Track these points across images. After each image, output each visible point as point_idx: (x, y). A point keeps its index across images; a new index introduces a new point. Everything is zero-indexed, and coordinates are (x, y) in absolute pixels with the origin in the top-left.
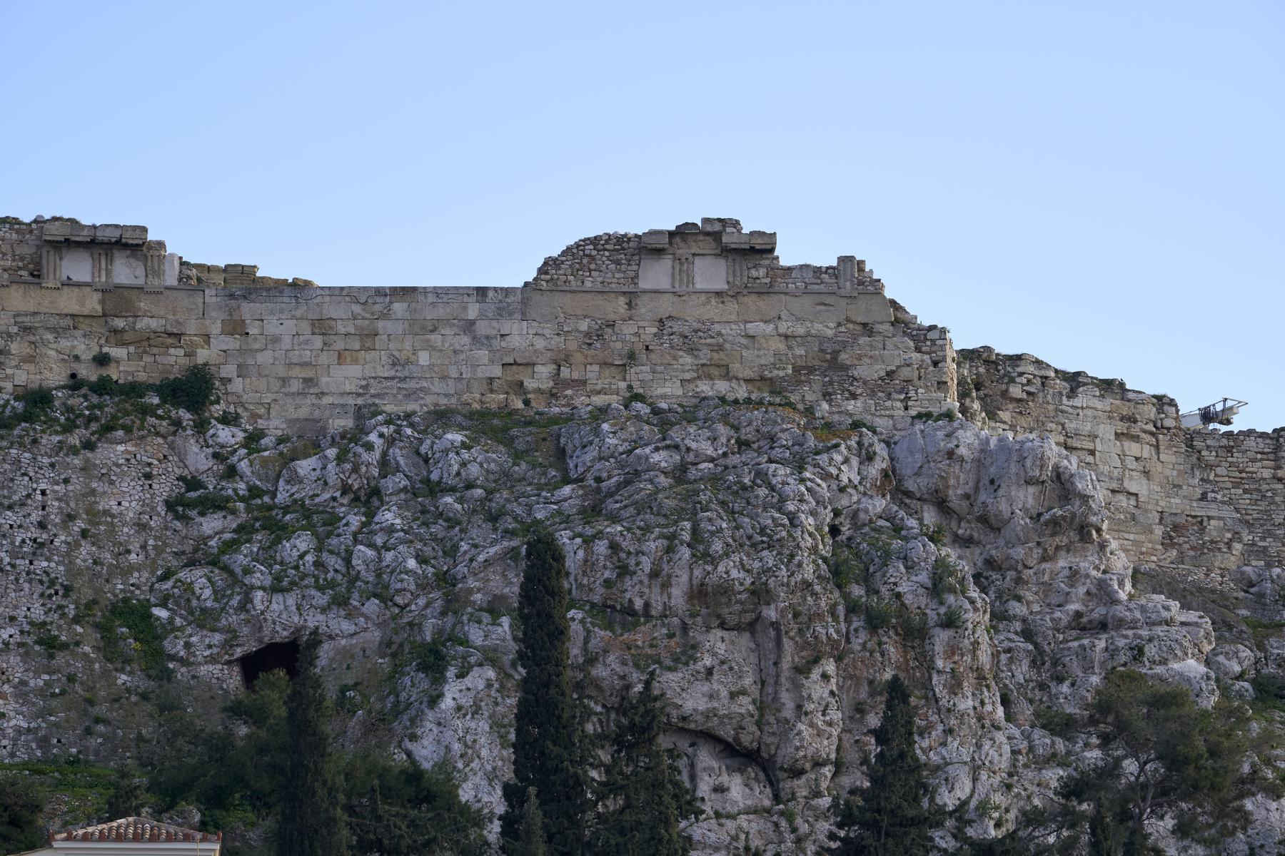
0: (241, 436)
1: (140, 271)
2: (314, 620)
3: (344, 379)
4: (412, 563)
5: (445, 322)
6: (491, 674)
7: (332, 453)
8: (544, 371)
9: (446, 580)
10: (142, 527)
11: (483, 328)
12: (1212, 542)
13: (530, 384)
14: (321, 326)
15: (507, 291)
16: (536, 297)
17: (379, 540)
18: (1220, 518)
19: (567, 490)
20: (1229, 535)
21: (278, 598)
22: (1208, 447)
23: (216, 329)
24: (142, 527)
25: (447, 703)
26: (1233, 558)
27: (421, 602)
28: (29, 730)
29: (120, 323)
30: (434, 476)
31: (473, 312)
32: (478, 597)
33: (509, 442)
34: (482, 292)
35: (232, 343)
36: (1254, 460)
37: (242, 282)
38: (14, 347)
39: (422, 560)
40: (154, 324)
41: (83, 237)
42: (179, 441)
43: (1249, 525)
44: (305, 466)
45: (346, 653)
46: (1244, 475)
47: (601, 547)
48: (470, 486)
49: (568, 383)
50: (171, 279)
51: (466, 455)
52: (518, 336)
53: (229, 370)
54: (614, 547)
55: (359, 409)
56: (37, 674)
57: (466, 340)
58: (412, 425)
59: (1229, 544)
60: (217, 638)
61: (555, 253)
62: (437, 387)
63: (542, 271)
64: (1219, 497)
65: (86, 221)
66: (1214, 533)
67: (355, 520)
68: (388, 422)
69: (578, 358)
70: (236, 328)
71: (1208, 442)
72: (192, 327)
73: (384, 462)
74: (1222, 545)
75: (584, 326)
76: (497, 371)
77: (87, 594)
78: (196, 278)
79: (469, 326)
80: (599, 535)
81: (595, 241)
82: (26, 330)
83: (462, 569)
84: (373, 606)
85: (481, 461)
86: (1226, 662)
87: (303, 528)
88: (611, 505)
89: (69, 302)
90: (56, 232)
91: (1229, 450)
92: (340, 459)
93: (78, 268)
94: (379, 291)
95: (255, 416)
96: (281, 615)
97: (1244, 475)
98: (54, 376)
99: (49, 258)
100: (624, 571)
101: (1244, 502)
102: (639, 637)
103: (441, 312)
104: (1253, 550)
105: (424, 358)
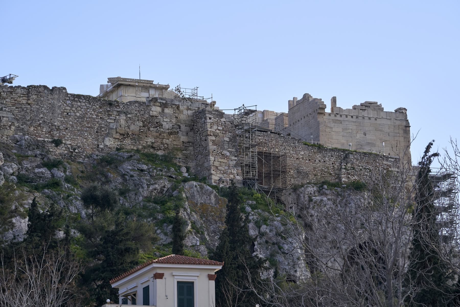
12: (4, 125)
18: (7, 117)
20: (10, 123)
22: (4, 91)
26: (11, 132)
36: (20, 97)
43: (18, 120)
46: (16, 102)
59: (10, 127)
64: (7, 109)
66: (5, 122)
71: (4, 90)
74: (7, 127)
86: (8, 169)
91: (11, 93)
97: (16, 102)
101: (16, 112)
104: (18, 129)
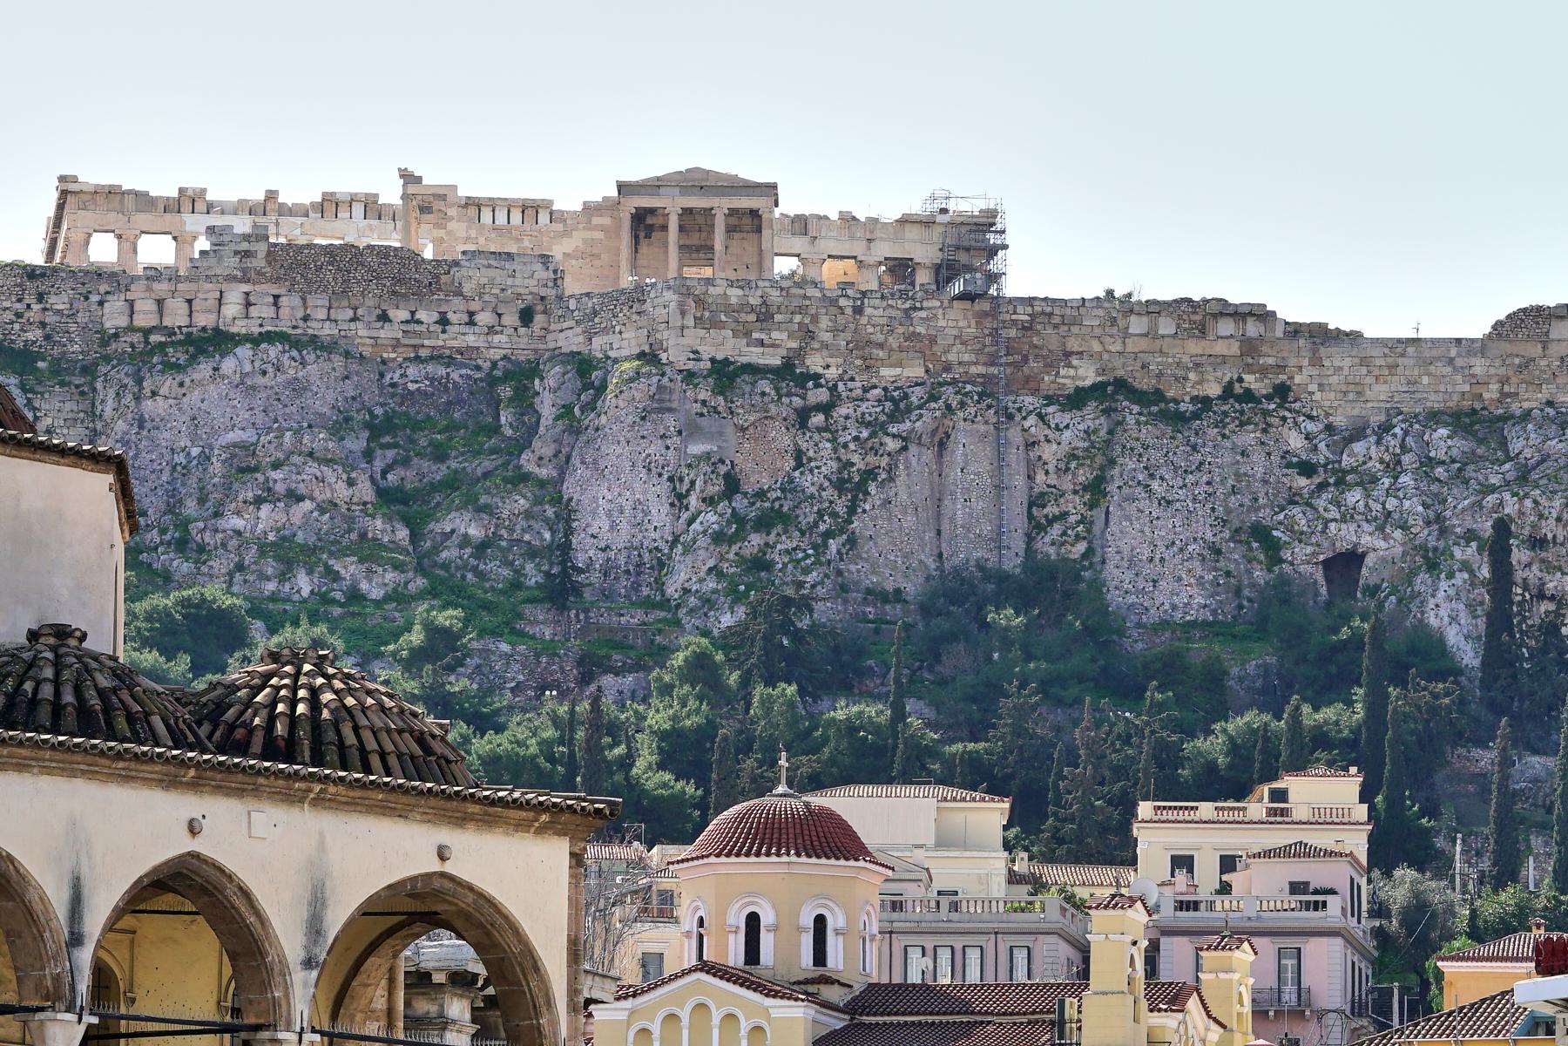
0: (1321, 426)
1: (1262, 329)
2: (1366, 540)
3: (1379, 392)
4: (1420, 509)
5: (1438, 359)
6: (1466, 576)
7: (1373, 439)
8: (1494, 387)
9: (1439, 518)
10: (1266, 482)
11: (1459, 362)
13: (1486, 396)
14: (1365, 361)
15: (1473, 341)
16: (1490, 344)
17: (1401, 494)
19: (1507, 466)
21: (1344, 526)
23: (1306, 362)
24: (1266, 482)
25: (1441, 594)
27: (1426, 532)
28: (1205, 606)
29: (1250, 360)
30: (1432, 454)
31: (1453, 353)
32: (1458, 530)
33: (1474, 434)
34: (1459, 341)
35: (1315, 372)
37: (1320, 335)
38: (1192, 376)
39: (1424, 504)
40: (1271, 361)
41: (1231, 310)
42: (1285, 430)
44: (1359, 447)
45: (1383, 559)
47: (1528, 503)
48: (1454, 461)
49: (1508, 395)
50: (1279, 333)
51: (1450, 442)
52: (1479, 366)
53: (1313, 387)
54: (1536, 502)
55: (1388, 410)
56: (1209, 571)
57: (1449, 369)
58: (1418, 422)
60: (1309, 550)
61: (1502, 317)
62: (1433, 397)
63: (1494, 327)
65: (1231, 301)
67: (1387, 481)
68: (1403, 421)
69: (1514, 380)
70: (1316, 361)
72: (1293, 362)
73: (1403, 446)
75: (1517, 361)
76: (1467, 388)
77: (1236, 523)
78: (1295, 330)
79: (1451, 361)
80: (1526, 496)
81: (1524, 310)
82: (1197, 365)
83: (1448, 513)
84: (1398, 534)
85: (1460, 445)
87: (1357, 484)
88: (1534, 476)
89: (1220, 348)
90: (1216, 309)
92: (1378, 443)
93: (1226, 327)
94: (1399, 341)
95: (1327, 415)
96: (1346, 535)
98: (1214, 390)
99: (1210, 323)
100: (1541, 516)
102: (1549, 555)
103: (1435, 353)
105: (1425, 380)
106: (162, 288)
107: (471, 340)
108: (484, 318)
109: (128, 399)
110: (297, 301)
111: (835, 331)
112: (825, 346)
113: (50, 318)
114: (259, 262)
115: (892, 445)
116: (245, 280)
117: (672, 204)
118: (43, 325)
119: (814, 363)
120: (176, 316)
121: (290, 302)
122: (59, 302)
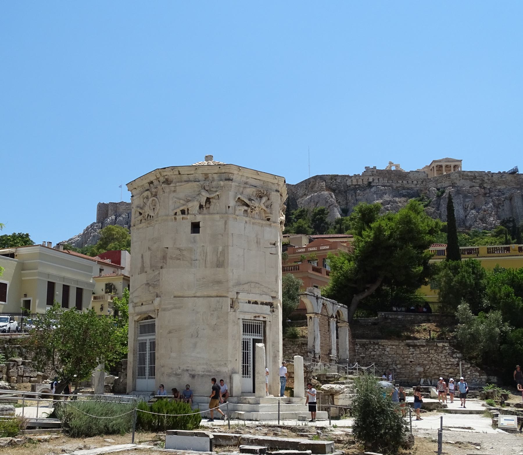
106: (357, 177)
107: (413, 186)
108: (415, 182)
109: (354, 196)
110: (382, 179)
111: (488, 179)
112: (486, 183)
113: (337, 183)
114: (375, 173)
115: (503, 199)
116: (373, 176)
117: (444, 164)
118: (336, 185)
119: (485, 185)
120: (360, 183)
121: (381, 179)
122: (339, 181)
